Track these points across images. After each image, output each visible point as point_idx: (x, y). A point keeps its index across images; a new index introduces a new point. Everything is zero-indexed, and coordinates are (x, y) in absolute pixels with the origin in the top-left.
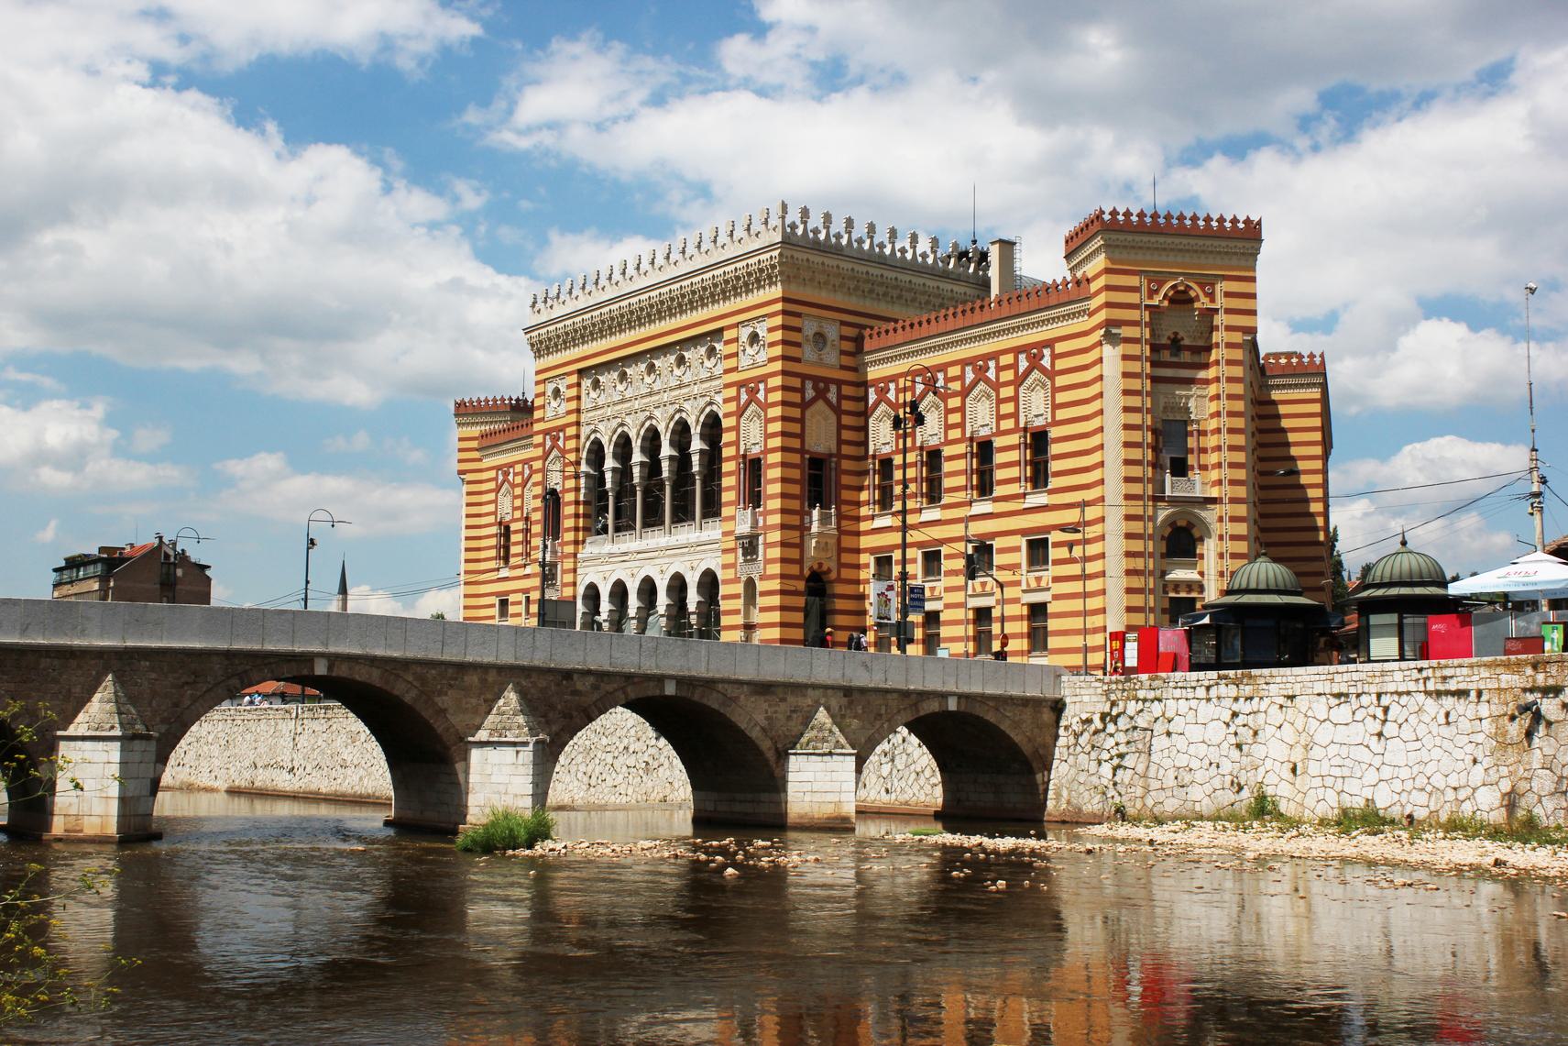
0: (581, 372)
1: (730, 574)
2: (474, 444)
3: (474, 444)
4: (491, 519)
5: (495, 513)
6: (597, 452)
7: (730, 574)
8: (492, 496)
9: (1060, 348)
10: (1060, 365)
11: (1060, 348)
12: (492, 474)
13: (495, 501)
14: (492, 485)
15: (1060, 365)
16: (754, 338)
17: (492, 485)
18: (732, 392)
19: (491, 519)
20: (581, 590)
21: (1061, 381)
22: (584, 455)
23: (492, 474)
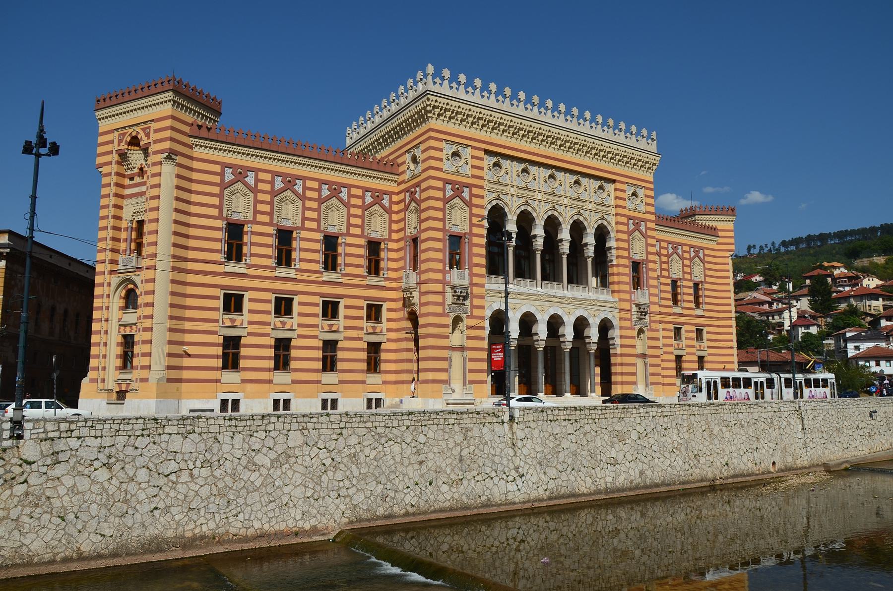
0: (487, 152)
1: (627, 324)
2: (187, 129)
3: (187, 129)
4: (215, 212)
5: (220, 207)
6: (497, 215)
7: (627, 324)
8: (216, 190)
9: (707, 252)
10: (707, 259)
11: (707, 252)
12: (217, 168)
13: (220, 196)
14: (217, 179)
15: (707, 259)
16: (634, 194)
17: (217, 179)
18: (625, 220)
19: (215, 212)
20: (488, 313)
21: (707, 266)
22: (486, 213)
23: (217, 168)
